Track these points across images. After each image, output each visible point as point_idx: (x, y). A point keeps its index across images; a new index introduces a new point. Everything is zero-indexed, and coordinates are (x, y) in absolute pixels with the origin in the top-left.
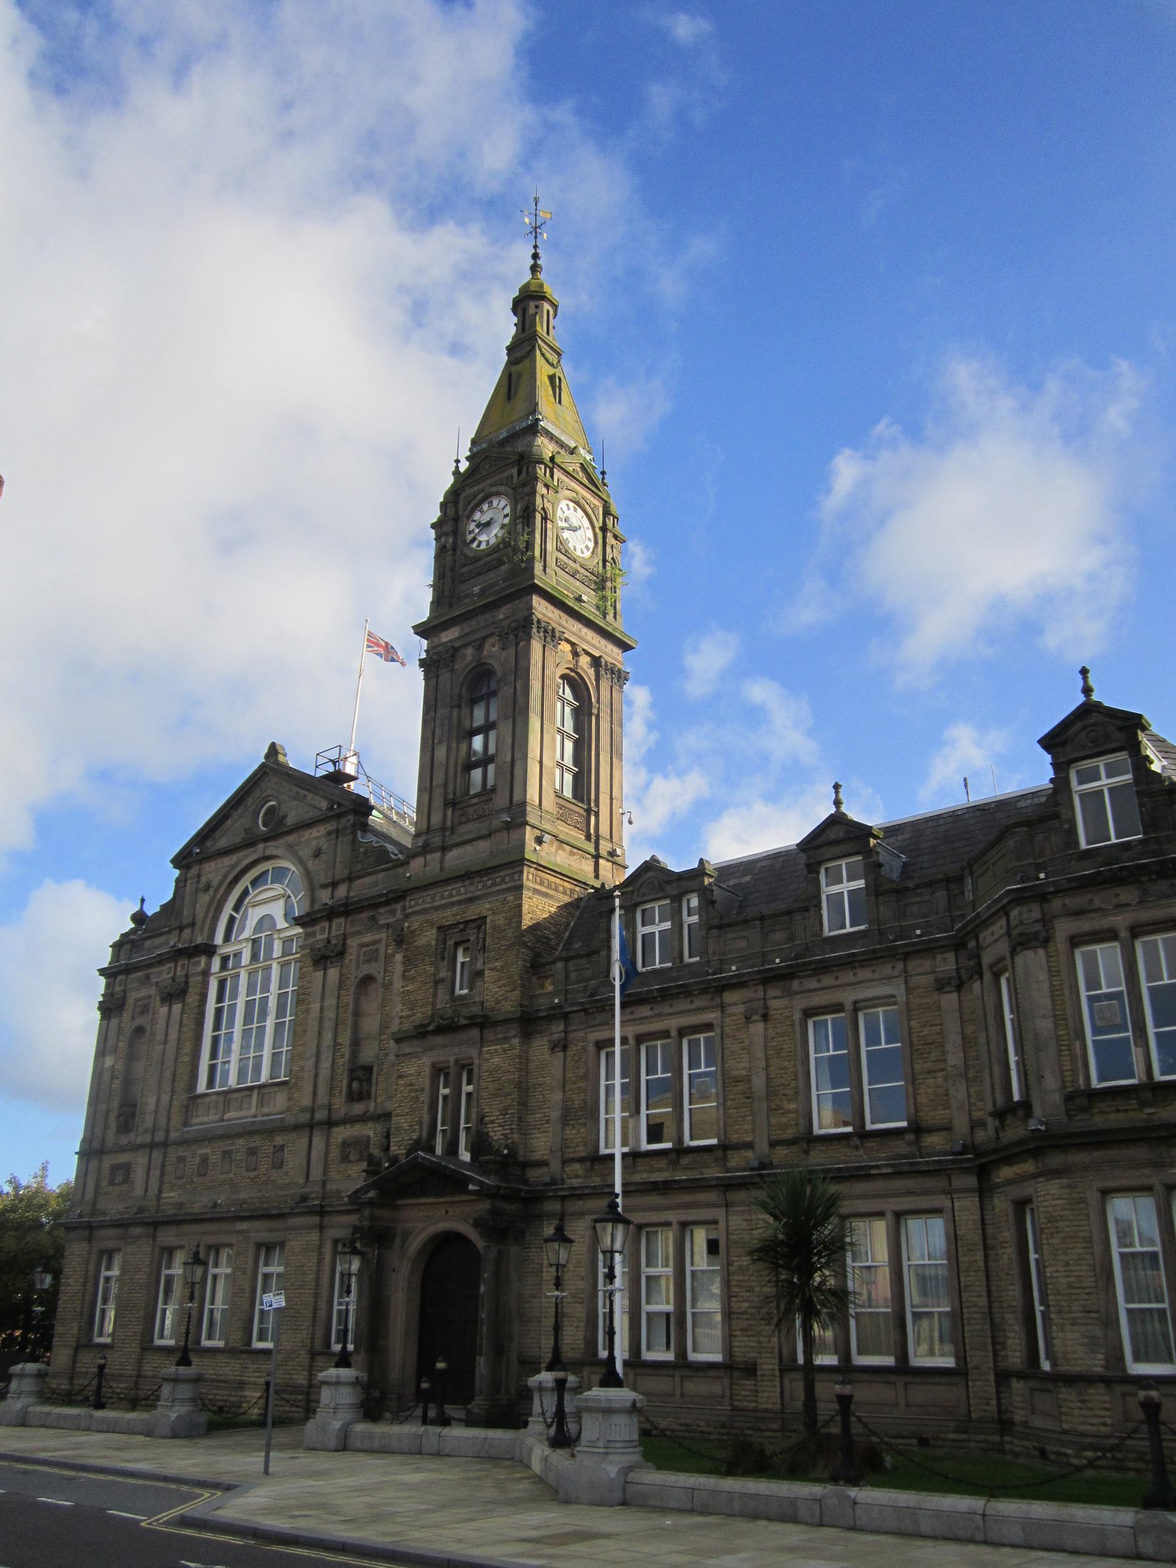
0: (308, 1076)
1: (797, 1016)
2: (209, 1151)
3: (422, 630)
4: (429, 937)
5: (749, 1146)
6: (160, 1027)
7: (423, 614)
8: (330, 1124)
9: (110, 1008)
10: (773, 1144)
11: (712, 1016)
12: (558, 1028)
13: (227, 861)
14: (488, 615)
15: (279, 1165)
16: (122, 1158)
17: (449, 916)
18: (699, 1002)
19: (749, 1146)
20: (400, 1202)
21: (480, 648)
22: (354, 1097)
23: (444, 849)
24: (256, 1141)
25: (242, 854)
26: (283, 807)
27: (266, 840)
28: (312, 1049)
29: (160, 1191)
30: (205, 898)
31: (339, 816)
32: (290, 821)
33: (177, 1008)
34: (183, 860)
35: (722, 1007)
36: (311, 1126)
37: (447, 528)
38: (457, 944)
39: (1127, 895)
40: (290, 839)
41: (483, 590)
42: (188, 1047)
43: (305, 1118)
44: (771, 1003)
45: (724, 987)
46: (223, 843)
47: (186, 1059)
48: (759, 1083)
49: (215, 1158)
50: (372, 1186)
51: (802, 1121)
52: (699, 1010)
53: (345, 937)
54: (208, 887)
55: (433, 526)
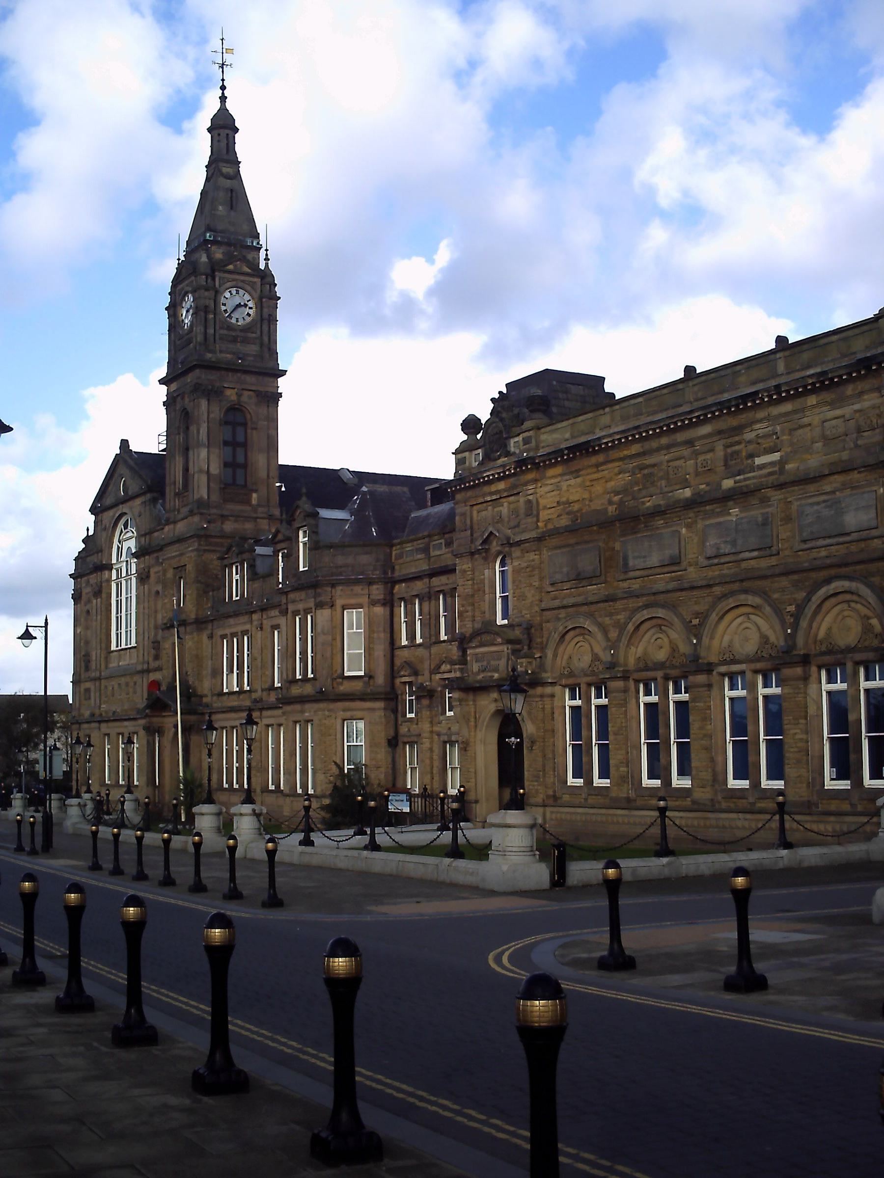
0: (141, 644)
1: (269, 630)
2: (113, 683)
3: (162, 382)
4: (170, 574)
5: (255, 691)
6: (94, 611)
7: (163, 372)
8: (148, 671)
9: (77, 597)
10: (263, 690)
11: (248, 627)
12: (210, 626)
13: (111, 513)
14: (182, 379)
15: (135, 692)
16: (88, 685)
17: (175, 563)
18: (246, 618)
19: (255, 691)
20: (164, 714)
21: (183, 398)
22: (157, 657)
23: (175, 522)
24: (128, 679)
25: (115, 509)
26: (128, 483)
27: (122, 503)
28: (141, 632)
29: (100, 704)
30: (104, 534)
31: (144, 494)
32: (130, 493)
33: (99, 600)
34: (93, 510)
35: (251, 622)
36: (142, 672)
37: (171, 312)
38: (181, 578)
39: (303, 595)
40: (130, 503)
41: (182, 363)
42: (104, 626)
43: (139, 668)
44: (265, 622)
45: (252, 612)
46: (109, 501)
47: (104, 631)
48: (259, 660)
49: (116, 687)
50: (147, 707)
51: (270, 681)
52: (245, 623)
53: (149, 568)
54: (105, 529)
55: (166, 309)
